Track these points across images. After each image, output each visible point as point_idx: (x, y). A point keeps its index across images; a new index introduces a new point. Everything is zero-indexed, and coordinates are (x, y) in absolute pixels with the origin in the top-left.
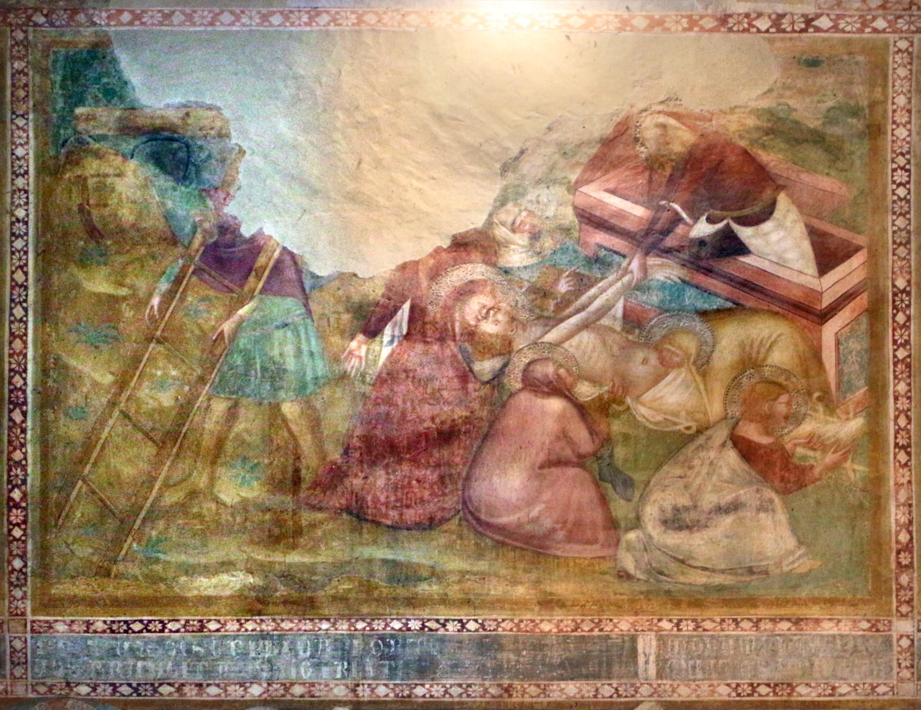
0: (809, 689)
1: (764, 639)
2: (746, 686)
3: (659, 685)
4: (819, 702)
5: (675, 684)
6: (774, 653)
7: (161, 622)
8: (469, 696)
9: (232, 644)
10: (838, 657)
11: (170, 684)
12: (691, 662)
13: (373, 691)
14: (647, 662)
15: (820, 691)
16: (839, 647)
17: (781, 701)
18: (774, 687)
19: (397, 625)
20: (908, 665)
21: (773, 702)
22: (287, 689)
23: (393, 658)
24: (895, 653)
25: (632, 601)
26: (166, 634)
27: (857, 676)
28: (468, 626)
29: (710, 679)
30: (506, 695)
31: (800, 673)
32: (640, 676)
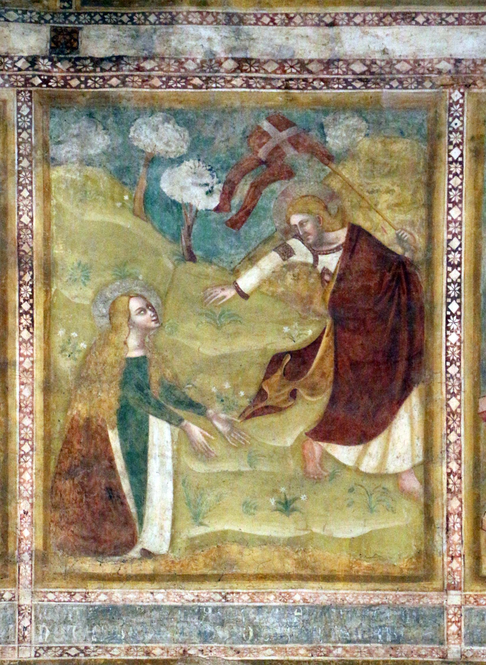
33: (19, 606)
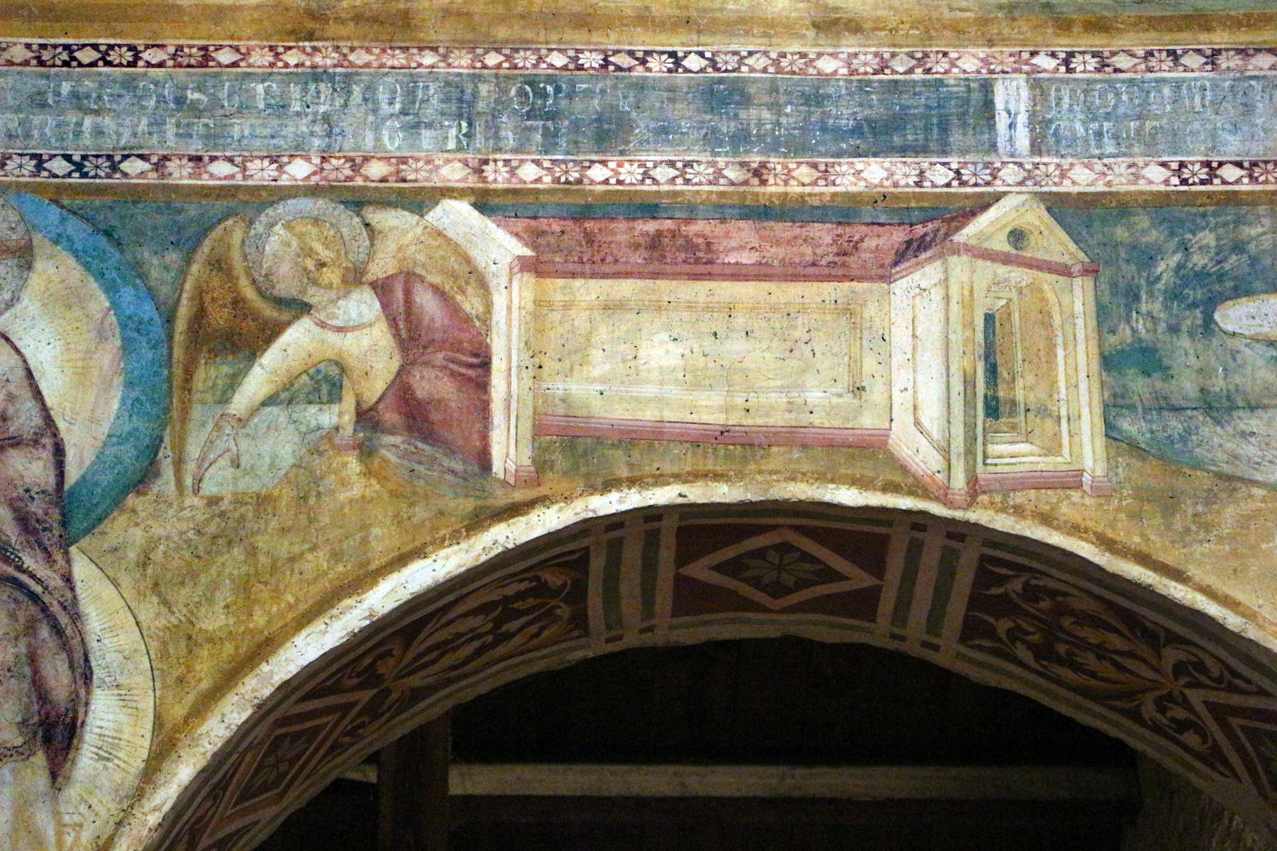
1: (1227, 83)
2: (1197, 166)
3: (1036, 166)
5: (1065, 163)
6: (1248, 109)
7: (131, 48)
8: (687, 182)
9: (260, 88)
11: (142, 157)
13: (512, 172)
14: (1012, 126)
17: (1266, 193)
18: (1251, 167)
19: (558, 60)
22: (356, 168)
23: (553, 116)
25: (983, 22)
26: (139, 70)
28: (685, 63)
29: (1131, 155)
30: (756, 181)
32: (1001, 150)
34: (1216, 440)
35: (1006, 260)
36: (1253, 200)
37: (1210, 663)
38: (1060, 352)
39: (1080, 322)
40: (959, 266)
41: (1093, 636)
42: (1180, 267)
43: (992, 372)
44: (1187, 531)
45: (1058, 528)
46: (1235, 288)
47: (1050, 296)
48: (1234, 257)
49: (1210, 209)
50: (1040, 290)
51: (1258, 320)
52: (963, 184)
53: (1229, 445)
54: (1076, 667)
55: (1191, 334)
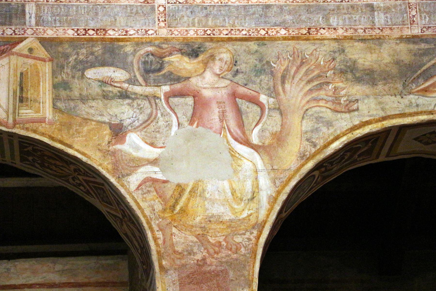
0: (115, 32)
1: (91, 7)
2: (82, 30)
4: (119, 38)
5: (45, 29)
6: (97, 14)
10: (128, 16)
12: (54, 18)
14: (30, 18)
15: (120, 33)
16: (129, 11)
17: (100, 38)
20: (163, 20)
21: (96, 38)
24: (157, 14)
27: (138, 26)
29: (64, 27)
31: (109, 24)
32: (27, 25)
33: (409, 3)
34: (83, 108)
35: (27, 57)
36: (97, 40)
37: (82, 170)
38: (41, 84)
39: (47, 75)
40: (14, 58)
41: (53, 162)
42: (76, 59)
43: (22, 89)
44: (74, 134)
45: (38, 134)
46: (91, 65)
47: (39, 67)
48: (91, 57)
49: (85, 42)
50: (37, 66)
51: (96, 75)
52: (16, 34)
53: (86, 110)
54: (51, 169)
55: (78, 79)
